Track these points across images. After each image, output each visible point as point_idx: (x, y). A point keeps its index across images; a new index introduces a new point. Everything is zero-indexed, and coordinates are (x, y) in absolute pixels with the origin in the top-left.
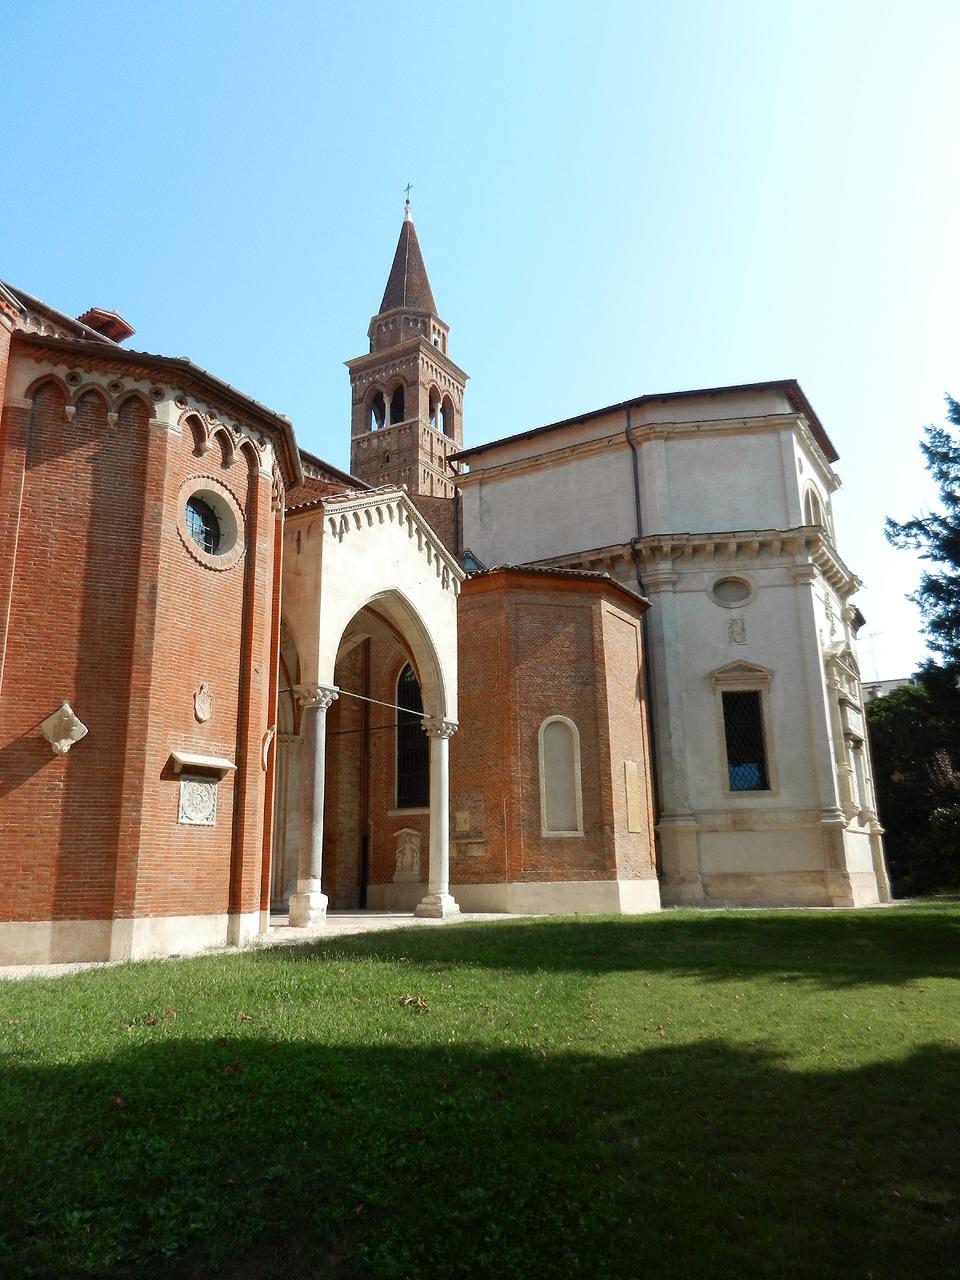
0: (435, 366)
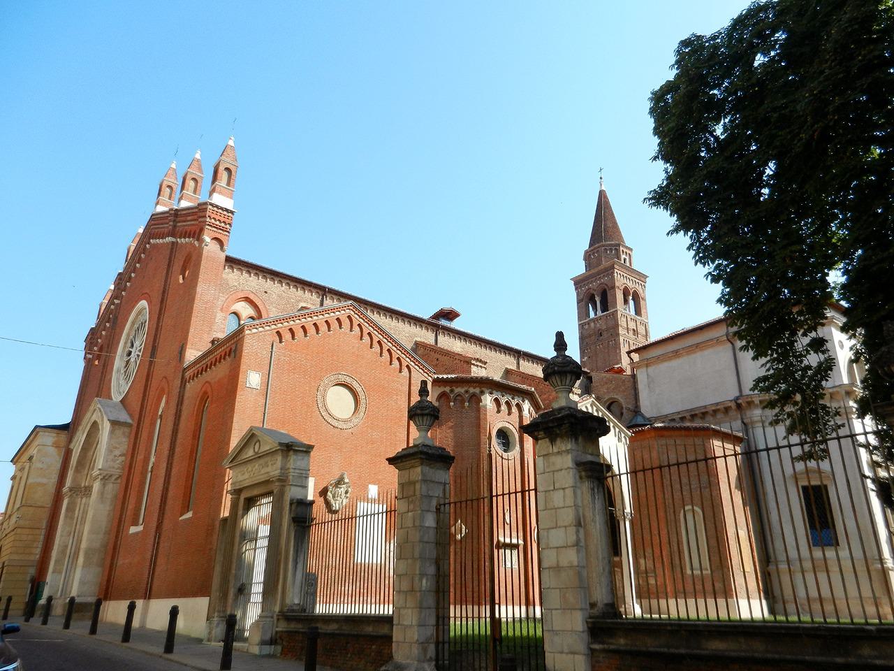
0: (625, 275)
